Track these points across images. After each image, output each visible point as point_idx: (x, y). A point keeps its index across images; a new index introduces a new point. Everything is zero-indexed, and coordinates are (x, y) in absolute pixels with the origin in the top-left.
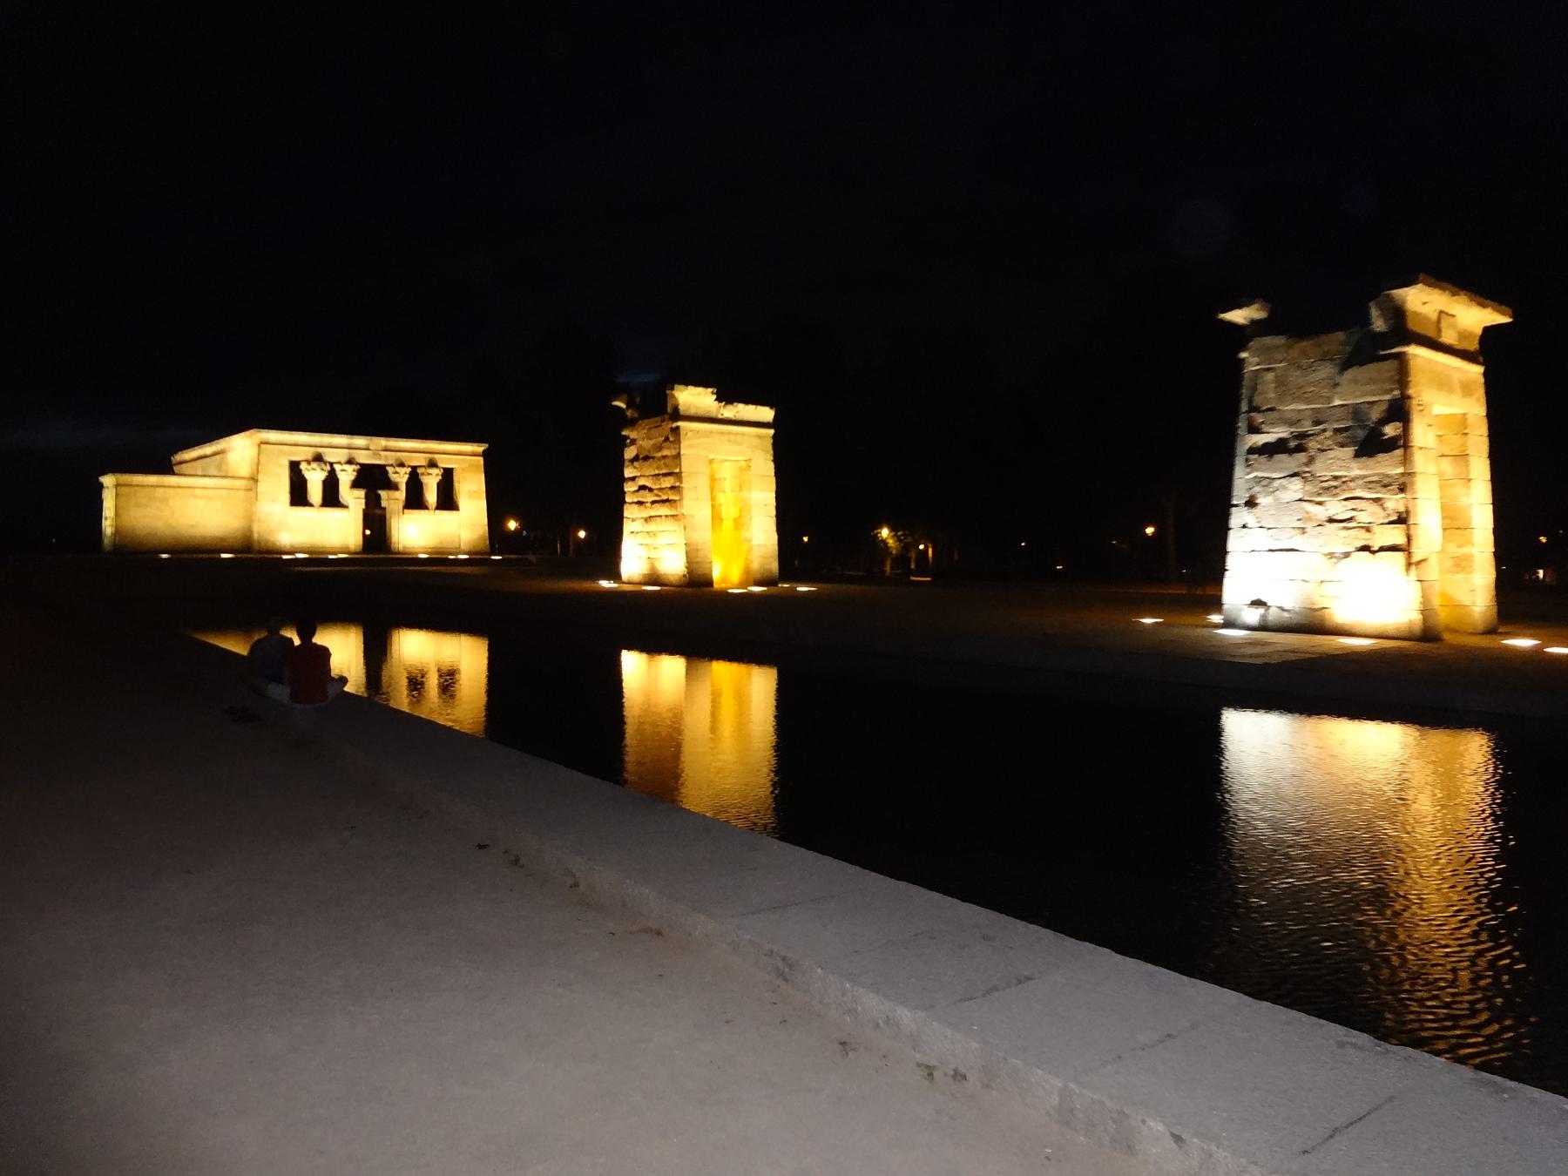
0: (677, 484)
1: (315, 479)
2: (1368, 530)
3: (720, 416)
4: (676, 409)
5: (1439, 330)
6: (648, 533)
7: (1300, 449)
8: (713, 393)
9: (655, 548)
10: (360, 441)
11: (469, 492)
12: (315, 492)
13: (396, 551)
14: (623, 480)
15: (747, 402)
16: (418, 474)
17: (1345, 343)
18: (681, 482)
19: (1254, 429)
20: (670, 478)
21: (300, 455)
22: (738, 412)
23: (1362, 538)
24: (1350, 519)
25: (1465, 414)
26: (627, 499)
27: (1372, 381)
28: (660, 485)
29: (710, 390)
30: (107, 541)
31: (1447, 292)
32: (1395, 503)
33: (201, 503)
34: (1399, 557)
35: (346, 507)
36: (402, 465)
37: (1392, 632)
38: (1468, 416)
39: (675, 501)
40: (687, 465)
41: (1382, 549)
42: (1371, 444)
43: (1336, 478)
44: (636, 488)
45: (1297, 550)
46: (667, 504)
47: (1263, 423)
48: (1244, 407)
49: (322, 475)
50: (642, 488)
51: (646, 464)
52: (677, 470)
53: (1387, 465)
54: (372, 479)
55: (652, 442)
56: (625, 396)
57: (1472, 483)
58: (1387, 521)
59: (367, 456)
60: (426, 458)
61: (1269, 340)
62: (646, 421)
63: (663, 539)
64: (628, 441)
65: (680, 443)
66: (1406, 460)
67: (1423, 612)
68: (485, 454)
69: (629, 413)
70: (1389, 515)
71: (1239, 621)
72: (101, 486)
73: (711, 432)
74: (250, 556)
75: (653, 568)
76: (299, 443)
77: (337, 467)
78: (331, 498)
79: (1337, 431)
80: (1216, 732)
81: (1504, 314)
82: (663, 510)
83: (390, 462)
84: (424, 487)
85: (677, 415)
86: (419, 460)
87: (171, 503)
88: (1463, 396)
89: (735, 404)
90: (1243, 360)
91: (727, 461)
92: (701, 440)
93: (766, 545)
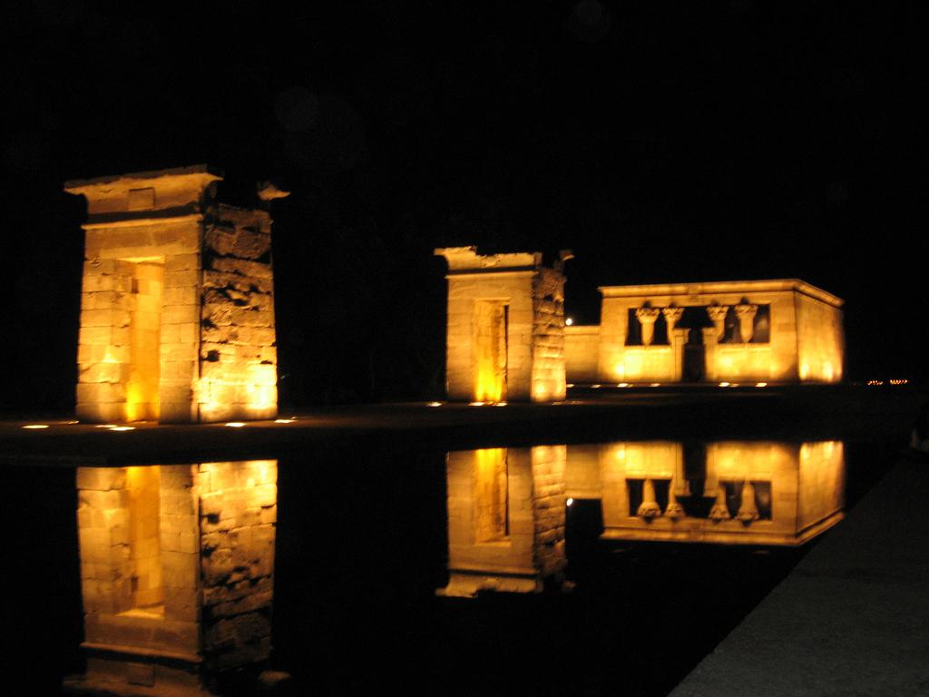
1: (647, 322)
8: (471, 250)
10: (680, 288)
12: (647, 333)
15: (506, 252)
16: (735, 312)
21: (635, 303)
29: (470, 247)
36: (716, 305)
54: (695, 320)
73: (474, 281)
77: (666, 311)
78: (660, 338)
83: (707, 303)
86: (733, 300)
88: (159, 245)
93: (521, 368)
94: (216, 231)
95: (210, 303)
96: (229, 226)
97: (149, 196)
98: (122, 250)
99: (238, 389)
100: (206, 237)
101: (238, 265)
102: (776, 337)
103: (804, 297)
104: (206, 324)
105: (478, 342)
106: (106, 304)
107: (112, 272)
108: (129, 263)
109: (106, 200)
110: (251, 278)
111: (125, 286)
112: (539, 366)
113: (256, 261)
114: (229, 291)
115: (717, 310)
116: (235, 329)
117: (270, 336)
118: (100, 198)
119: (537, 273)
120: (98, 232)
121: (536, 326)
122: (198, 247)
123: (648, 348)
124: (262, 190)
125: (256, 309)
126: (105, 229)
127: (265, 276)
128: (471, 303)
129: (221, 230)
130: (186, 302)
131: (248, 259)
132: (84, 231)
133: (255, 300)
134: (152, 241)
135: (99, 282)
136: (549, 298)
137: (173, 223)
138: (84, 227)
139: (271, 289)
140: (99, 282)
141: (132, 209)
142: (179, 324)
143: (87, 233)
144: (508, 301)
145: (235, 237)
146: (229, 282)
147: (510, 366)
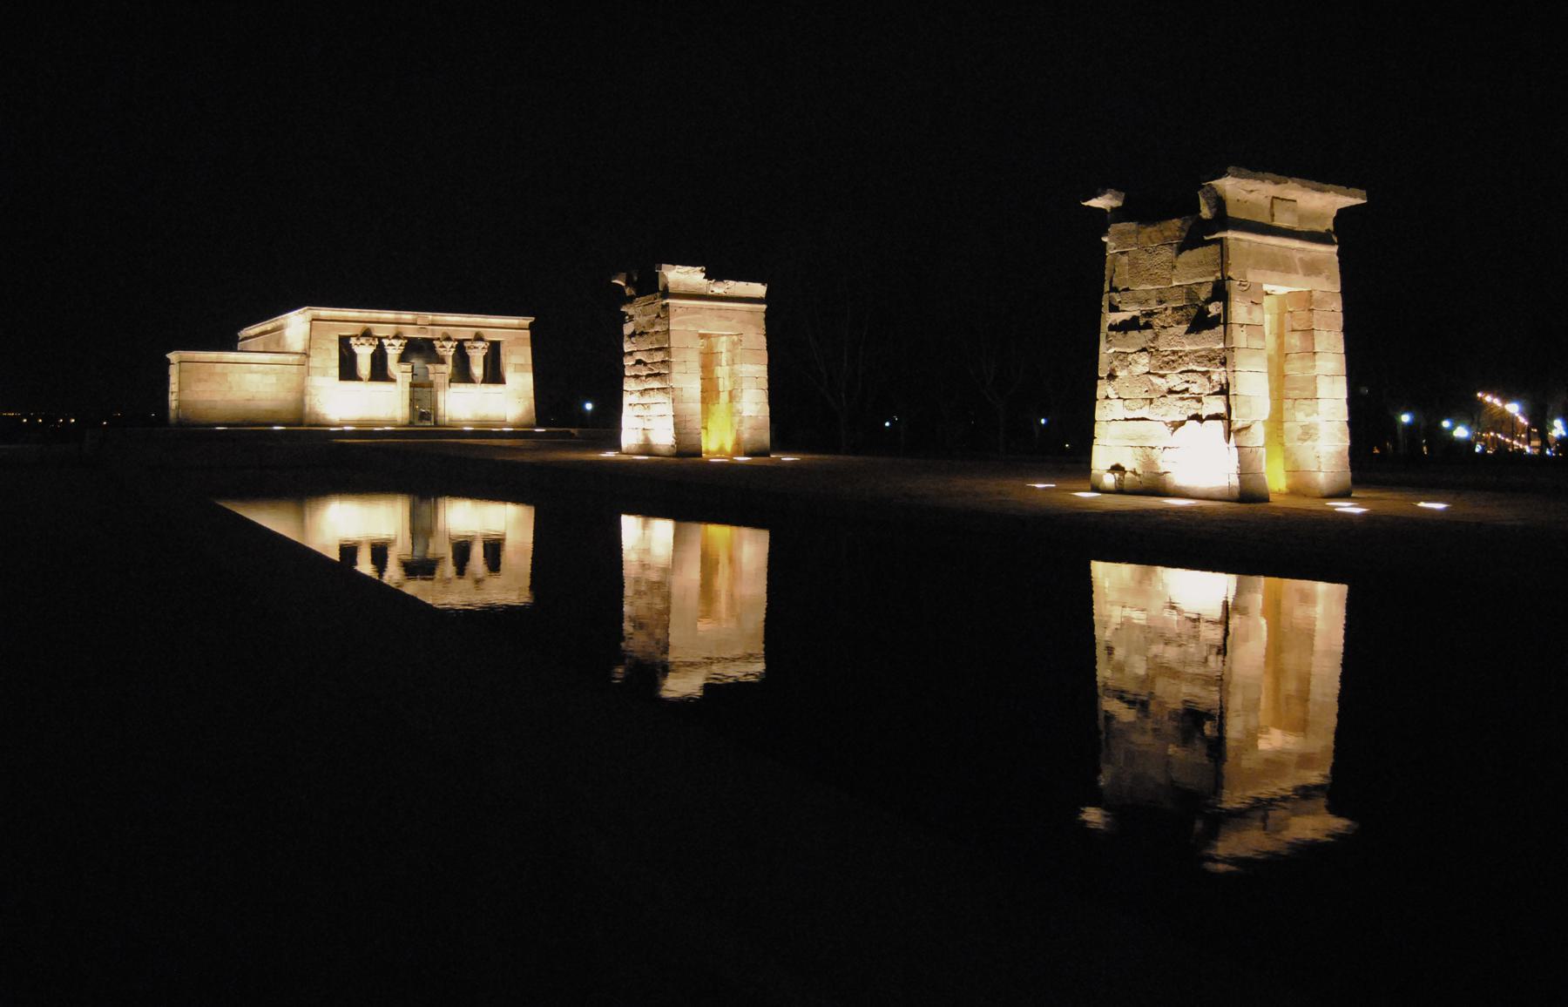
0: (667, 359)
1: (364, 353)
2: (1199, 400)
3: (710, 293)
4: (666, 287)
5: (1273, 215)
6: (643, 405)
7: (1148, 326)
8: (702, 271)
9: (649, 420)
10: (407, 316)
12: (364, 366)
13: (443, 423)
14: (623, 354)
15: (738, 279)
16: (464, 348)
17: (1181, 229)
18: (670, 356)
19: (1114, 309)
20: (660, 353)
21: (349, 330)
23: (1194, 408)
24: (1187, 390)
25: (1310, 291)
26: (627, 373)
27: (1200, 263)
28: (653, 359)
29: (700, 268)
30: (172, 415)
31: (1267, 181)
32: (1218, 375)
33: (255, 378)
34: (1219, 426)
35: (393, 381)
36: (448, 339)
37: (1217, 495)
38: (1314, 293)
39: (665, 374)
40: (674, 342)
41: (1210, 418)
42: (1200, 323)
43: (1174, 352)
44: (633, 363)
45: (1148, 420)
46: (658, 377)
47: (1120, 302)
48: (1107, 288)
49: (372, 349)
50: (639, 362)
51: (641, 339)
52: (667, 346)
53: (1209, 341)
55: (646, 318)
56: (624, 275)
57: (1317, 356)
58: (1211, 392)
60: (472, 331)
61: (1122, 226)
62: (642, 298)
63: (655, 410)
64: (627, 317)
65: (669, 320)
66: (1226, 336)
67: (1240, 475)
68: (531, 327)
69: (628, 291)
70: (1213, 387)
71: (1101, 486)
72: (168, 363)
73: (701, 308)
74: (302, 428)
75: (647, 439)
77: (386, 342)
78: (380, 372)
79: (1175, 309)
80: (1084, 589)
81: (1355, 197)
82: (655, 384)
83: (436, 336)
84: (471, 359)
85: (666, 294)
86: (467, 333)
87: (229, 379)
88: (1305, 275)
90: (1105, 243)
91: (723, 335)
98: (1269, 273)
102: (509, 374)
109: (1246, 202)
115: (449, 344)
118: (1239, 198)
126: (1249, 241)
134: (1300, 271)
137: (1315, 251)
140: (1250, 312)
141: (1277, 223)
143: (1230, 242)
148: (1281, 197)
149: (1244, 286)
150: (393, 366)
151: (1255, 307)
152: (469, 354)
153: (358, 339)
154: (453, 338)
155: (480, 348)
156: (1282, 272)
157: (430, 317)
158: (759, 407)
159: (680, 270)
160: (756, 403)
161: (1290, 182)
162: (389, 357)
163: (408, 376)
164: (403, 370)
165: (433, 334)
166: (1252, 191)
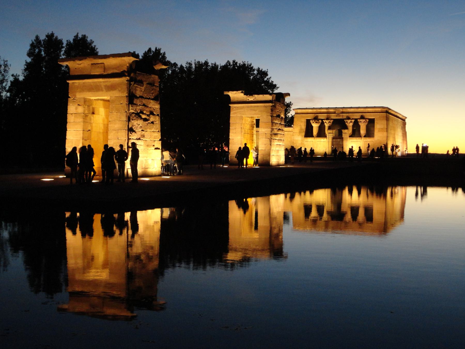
1: (315, 126)
3: (248, 100)
8: (242, 92)
11: (379, 129)
12: (315, 132)
15: (258, 94)
16: (358, 122)
21: (310, 117)
22: (255, 98)
29: (241, 91)
36: (348, 118)
59: (335, 115)
76: (309, 113)
78: (321, 134)
86: (357, 116)
88: (107, 91)
89: (253, 95)
92: (239, 111)
94: (135, 85)
95: (133, 120)
96: (140, 83)
97: (101, 67)
98: (88, 93)
99: (144, 161)
100: (130, 88)
101: (144, 101)
103: (390, 115)
104: (131, 130)
105: (244, 137)
106: (80, 120)
107: (83, 104)
108: (90, 100)
109: (79, 68)
110: (151, 107)
111: (89, 110)
112: (274, 148)
113: (152, 99)
114: (140, 114)
115: (349, 121)
116: (143, 132)
117: (158, 135)
118: (76, 67)
119: (273, 104)
120: (75, 84)
121: (272, 129)
122: (127, 93)
123: (316, 138)
124: (155, 65)
125: (152, 123)
126: (79, 83)
127: (156, 106)
128: (242, 118)
129: (137, 85)
130: (121, 120)
131: (149, 99)
132: (68, 83)
133: (152, 119)
134: (104, 90)
135: (76, 109)
136: (278, 116)
137: (114, 81)
138: (68, 82)
139: (159, 113)
140: (76, 109)
142: (118, 130)
143: (69, 84)
144: (258, 117)
145: (143, 88)
146: (141, 110)
147: (259, 149)
148: (95, 63)
149: (75, 99)
150: (327, 131)
151: (79, 107)
152: (360, 124)
153: (312, 121)
154: (351, 118)
155: (362, 122)
156: (94, 91)
157: (341, 110)
158: (266, 146)
159: (232, 93)
160: (265, 144)
161: (88, 58)
162: (326, 127)
163: (331, 135)
164: (329, 132)
165: (343, 117)
166: (81, 64)
